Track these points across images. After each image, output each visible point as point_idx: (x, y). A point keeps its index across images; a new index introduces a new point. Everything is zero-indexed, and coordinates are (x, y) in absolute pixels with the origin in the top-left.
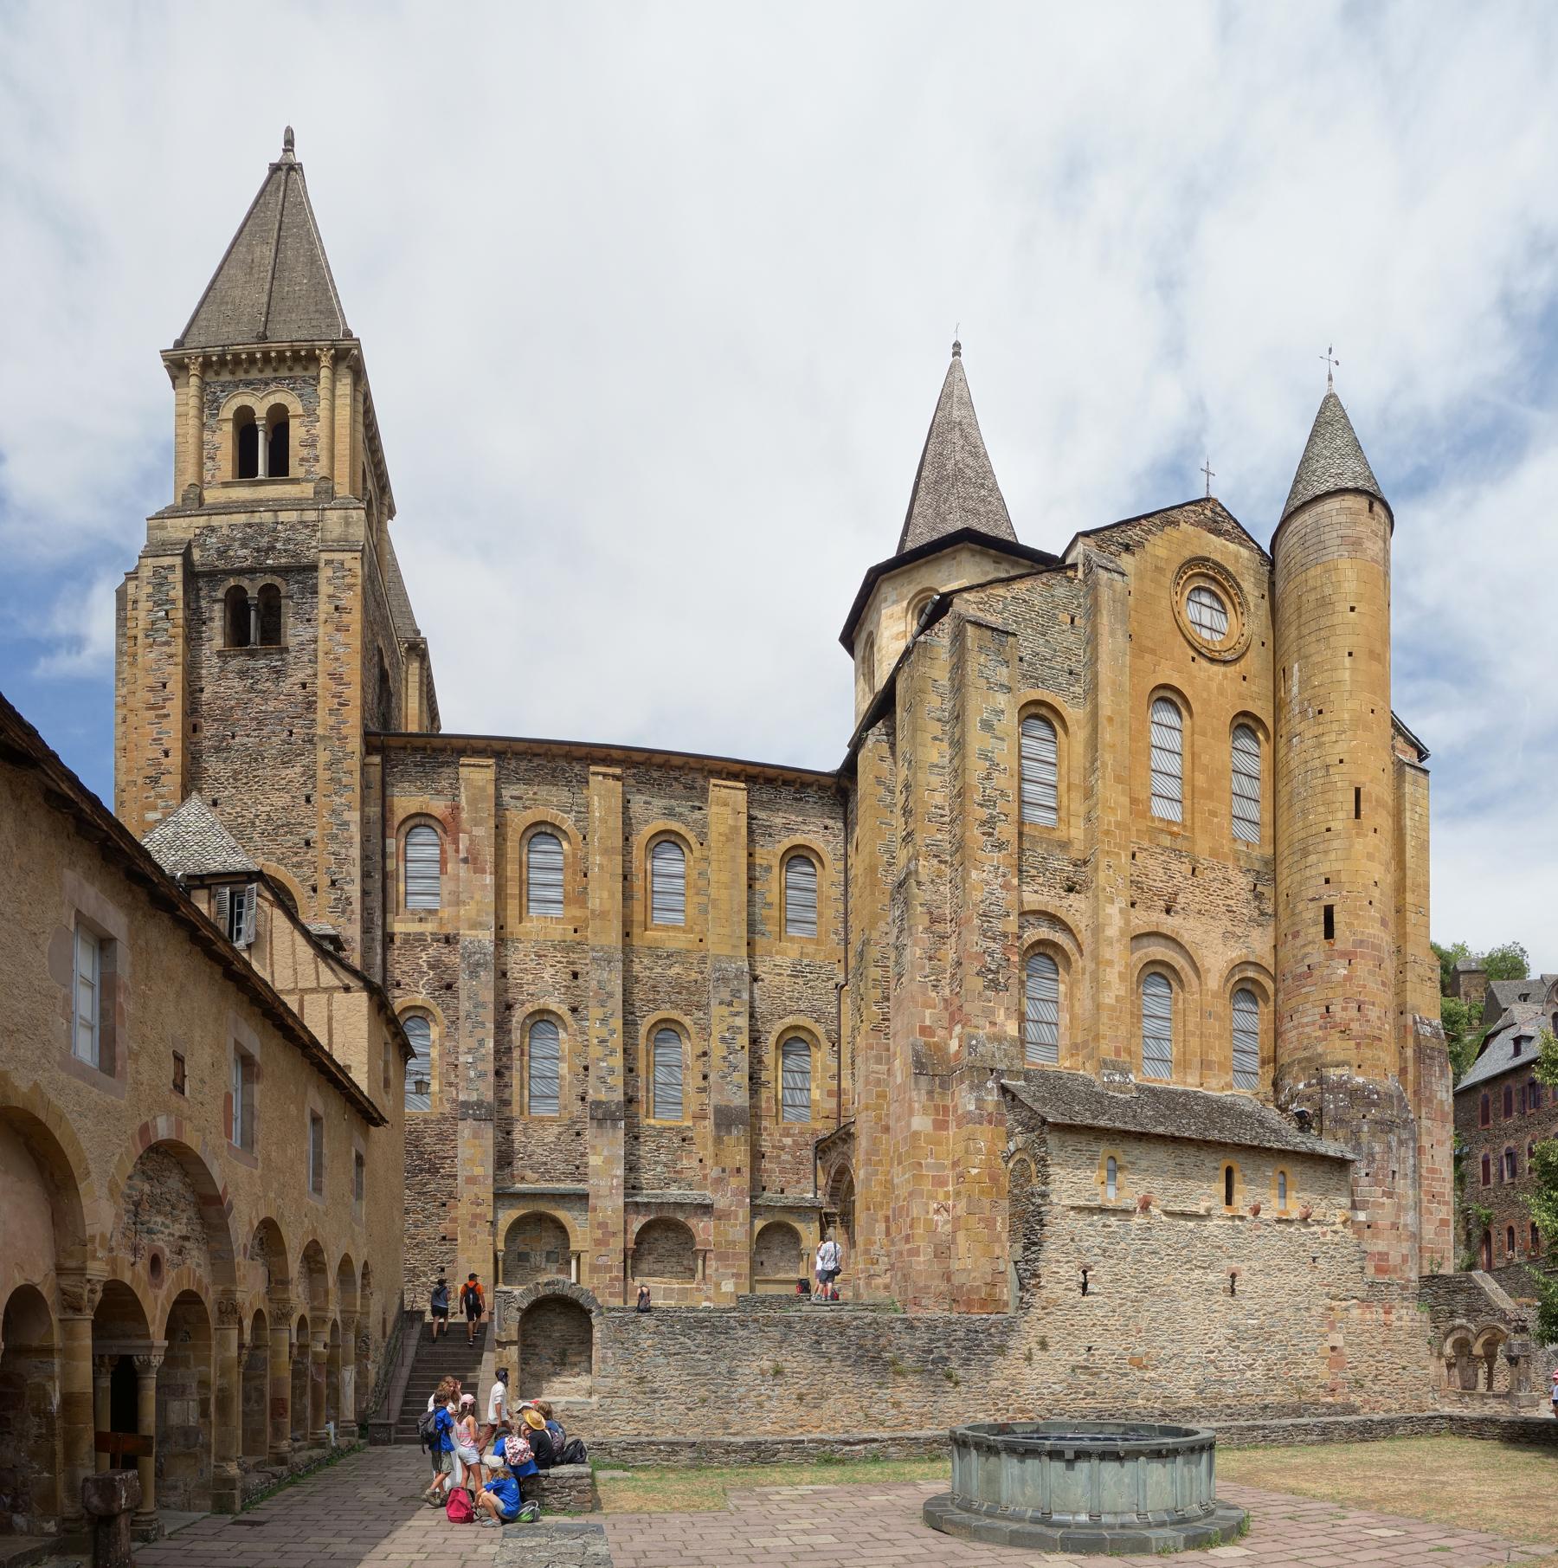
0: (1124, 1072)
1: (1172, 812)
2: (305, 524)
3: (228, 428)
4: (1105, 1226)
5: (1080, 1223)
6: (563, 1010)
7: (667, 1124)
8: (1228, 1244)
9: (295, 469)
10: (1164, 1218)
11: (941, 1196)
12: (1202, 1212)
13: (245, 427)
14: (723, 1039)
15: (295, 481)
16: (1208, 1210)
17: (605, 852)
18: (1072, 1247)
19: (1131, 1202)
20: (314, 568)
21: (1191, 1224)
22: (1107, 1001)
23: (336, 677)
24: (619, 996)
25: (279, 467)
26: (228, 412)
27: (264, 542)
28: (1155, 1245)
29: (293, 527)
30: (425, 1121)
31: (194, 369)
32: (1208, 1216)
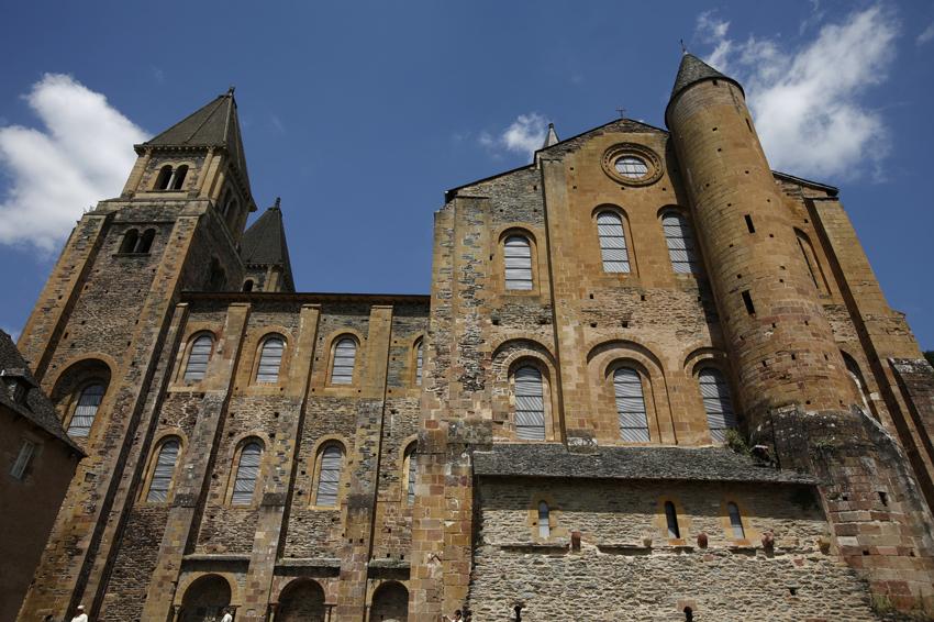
0: (588, 437)
1: (624, 268)
2: (178, 207)
3: (157, 172)
4: (536, 563)
5: (512, 560)
6: (265, 436)
7: (322, 509)
8: (675, 576)
9: (184, 187)
10: (599, 553)
11: (435, 548)
12: (642, 545)
13: (166, 172)
14: (361, 450)
15: (183, 191)
16: (648, 542)
17: (304, 345)
18: (504, 584)
19: (563, 539)
20: (173, 223)
21: (630, 558)
22: (569, 388)
23: (169, 267)
24: (296, 426)
25: (178, 186)
26: (160, 167)
27: (155, 213)
28: (592, 581)
29: (171, 207)
30: (158, 509)
31: (149, 152)
32: (648, 550)
